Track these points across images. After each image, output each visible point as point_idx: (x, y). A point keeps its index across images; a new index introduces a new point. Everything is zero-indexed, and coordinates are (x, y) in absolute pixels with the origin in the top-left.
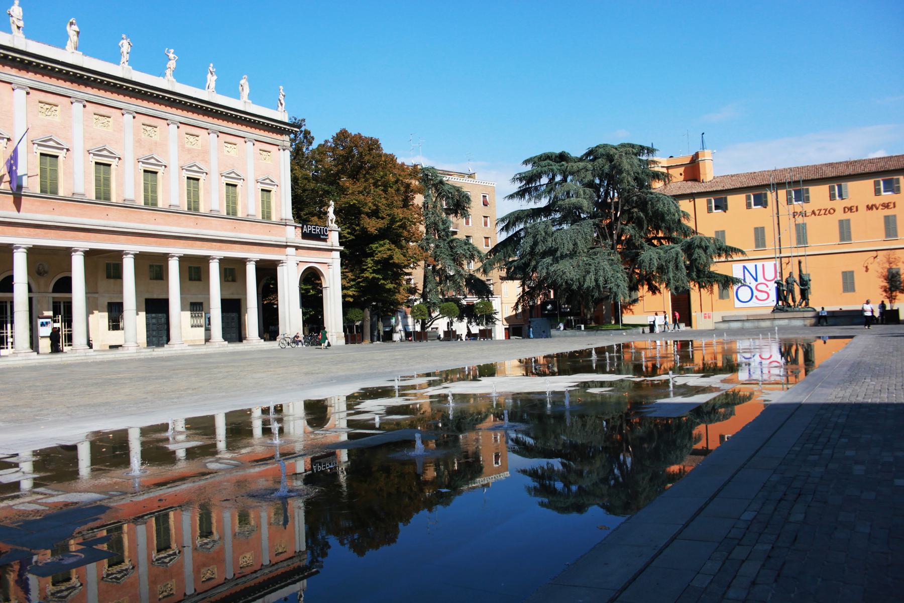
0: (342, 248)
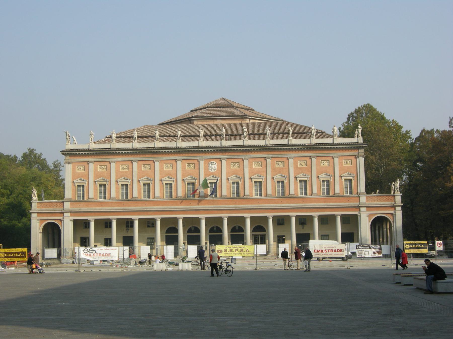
0: (402, 205)
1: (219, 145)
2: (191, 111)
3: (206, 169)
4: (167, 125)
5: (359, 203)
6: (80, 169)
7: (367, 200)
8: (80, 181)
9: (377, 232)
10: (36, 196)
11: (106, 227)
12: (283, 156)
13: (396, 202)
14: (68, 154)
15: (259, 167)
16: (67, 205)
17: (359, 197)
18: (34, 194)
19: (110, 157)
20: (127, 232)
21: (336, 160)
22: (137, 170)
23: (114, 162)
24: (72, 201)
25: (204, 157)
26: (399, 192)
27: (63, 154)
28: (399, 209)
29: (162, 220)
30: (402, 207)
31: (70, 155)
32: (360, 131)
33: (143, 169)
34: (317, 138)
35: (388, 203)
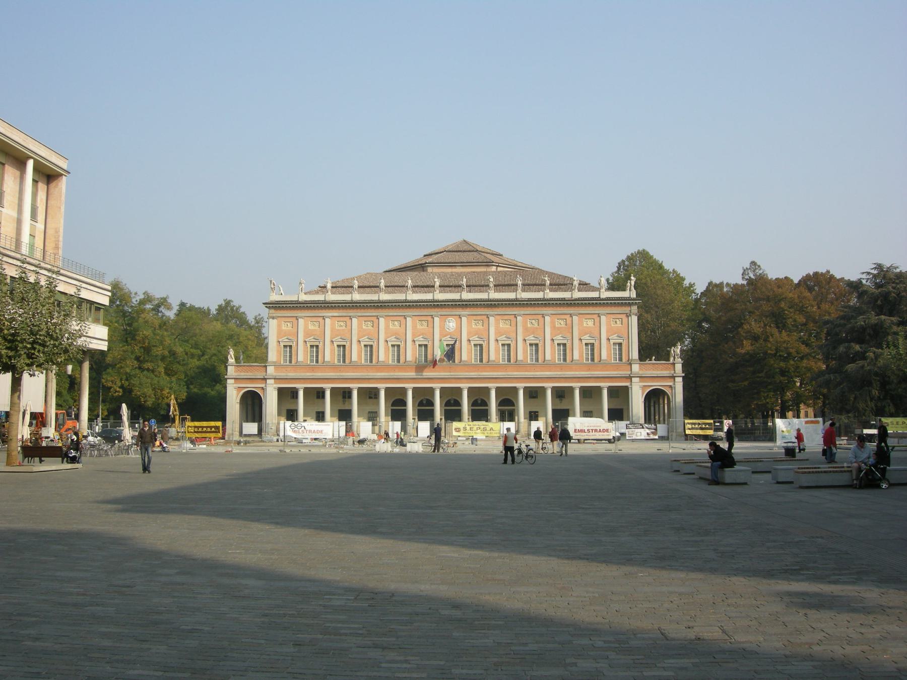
0: (684, 375)
1: (459, 298)
2: (425, 256)
3: (442, 328)
4: (395, 273)
5: (630, 372)
6: (287, 325)
7: (640, 369)
8: (287, 340)
9: (652, 409)
10: (233, 358)
11: (318, 397)
12: (537, 312)
13: (676, 372)
14: (272, 306)
15: (507, 326)
16: (271, 370)
17: (630, 364)
18: (231, 356)
19: (324, 311)
20: (344, 404)
21: (603, 318)
22: (356, 327)
23: (328, 317)
24: (277, 366)
25: (439, 313)
26: (680, 360)
27: (266, 307)
28: (679, 380)
29: (387, 390)
30: (683, 377)
31: (275, 308)
32: (633, 283)
33: (364, 327)
34: (579, 290)
35: (666, 373)
